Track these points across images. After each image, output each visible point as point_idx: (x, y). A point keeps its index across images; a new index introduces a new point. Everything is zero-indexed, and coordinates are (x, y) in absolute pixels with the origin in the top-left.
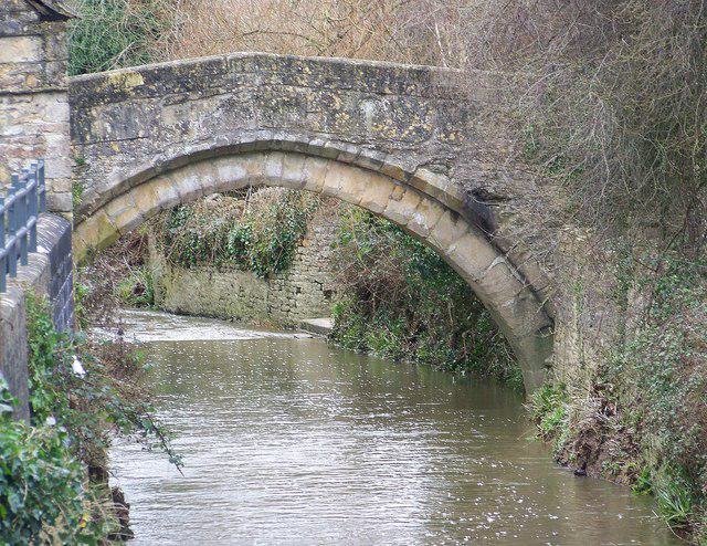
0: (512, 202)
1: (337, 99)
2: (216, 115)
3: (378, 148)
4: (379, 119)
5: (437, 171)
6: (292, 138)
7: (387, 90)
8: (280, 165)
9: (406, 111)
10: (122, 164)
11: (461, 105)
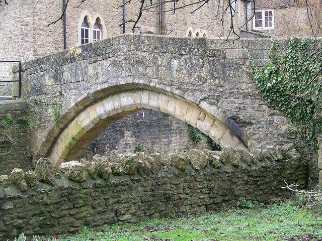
0: (254, 126)
1: (159, 59)
2: (109, 69)
3: (179, 88)
4: (179, 70)
5: (211, 104)
6: (141, 82)
7: (183, 52)
8: (148, 97)
9: (193, 65)
10: (75, 95)
11: (222, 61)
